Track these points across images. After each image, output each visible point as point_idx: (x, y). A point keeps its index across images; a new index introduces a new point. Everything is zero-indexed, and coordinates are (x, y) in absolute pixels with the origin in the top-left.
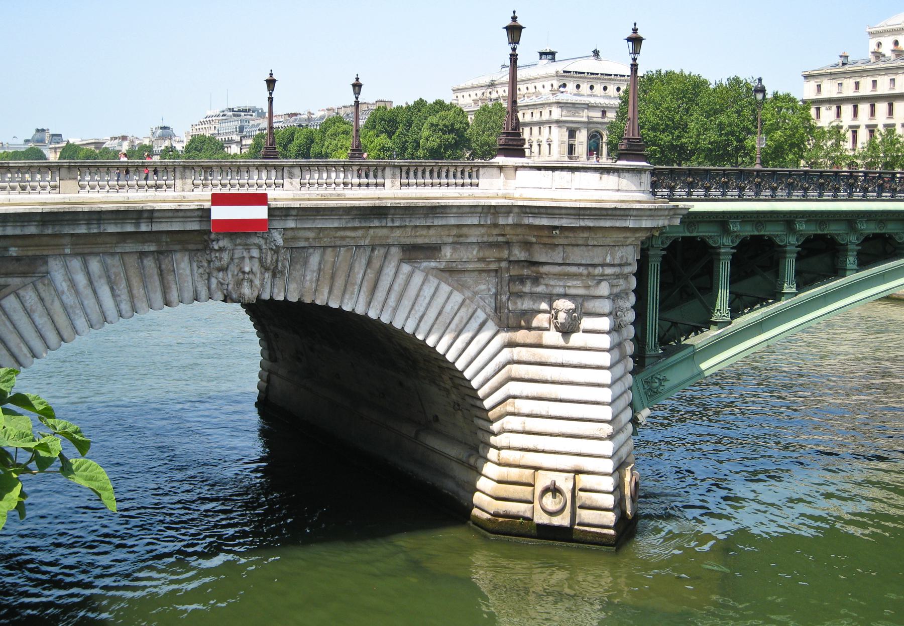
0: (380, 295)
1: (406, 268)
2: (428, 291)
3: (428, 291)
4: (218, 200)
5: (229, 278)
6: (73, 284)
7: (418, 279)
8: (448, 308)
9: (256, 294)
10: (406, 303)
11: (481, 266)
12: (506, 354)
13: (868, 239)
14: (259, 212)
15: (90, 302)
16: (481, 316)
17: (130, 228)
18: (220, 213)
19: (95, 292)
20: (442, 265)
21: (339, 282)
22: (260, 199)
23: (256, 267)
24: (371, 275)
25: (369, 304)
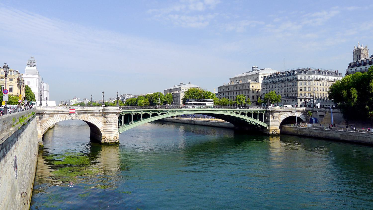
0: (88, 119)
1: (91, 116)
2: (94, 119)
3: (94, 119)
5: (72, 117)
12: (103, 125)
16: (100, 121)
22: (74, 110)
23: (75, 116)
25: (87, 120)
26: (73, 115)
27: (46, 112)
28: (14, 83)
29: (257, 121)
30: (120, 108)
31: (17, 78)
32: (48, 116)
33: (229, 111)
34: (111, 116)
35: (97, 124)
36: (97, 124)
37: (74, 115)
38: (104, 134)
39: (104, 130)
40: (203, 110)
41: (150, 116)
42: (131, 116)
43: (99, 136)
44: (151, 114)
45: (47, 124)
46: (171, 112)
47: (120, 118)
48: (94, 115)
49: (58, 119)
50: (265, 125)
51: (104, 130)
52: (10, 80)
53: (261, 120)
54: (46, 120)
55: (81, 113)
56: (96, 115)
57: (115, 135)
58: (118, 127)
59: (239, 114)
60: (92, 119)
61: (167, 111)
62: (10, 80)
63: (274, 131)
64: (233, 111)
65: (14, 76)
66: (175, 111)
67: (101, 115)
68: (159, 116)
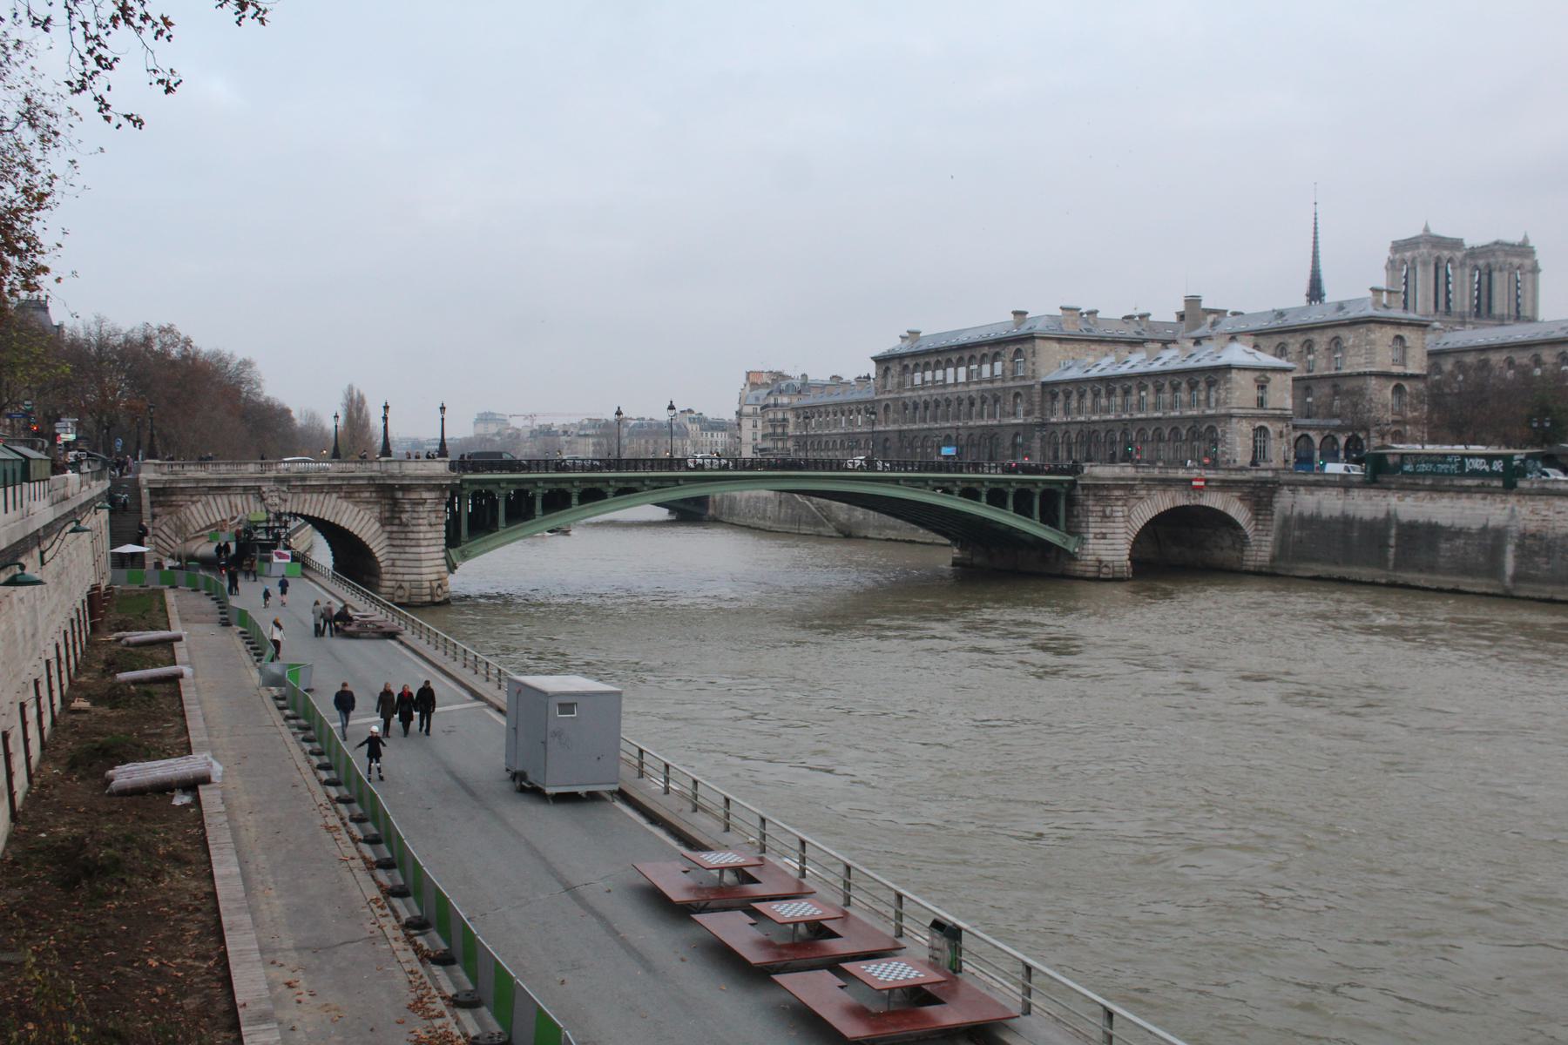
29: (1032, 524)
30: (452, 467)
33: (906, 479)
40: (795, 477)
41: (575, 500)
43: (374, 580)
44: (575, 492)
50: (1071, 546)
53: (1049, 519)
56: (357, 495)
58: (444, 541)
59: (951, 492)
61: (641, 480)
63: (1106, 566)
64: (925, 480)
66: (676, 480)
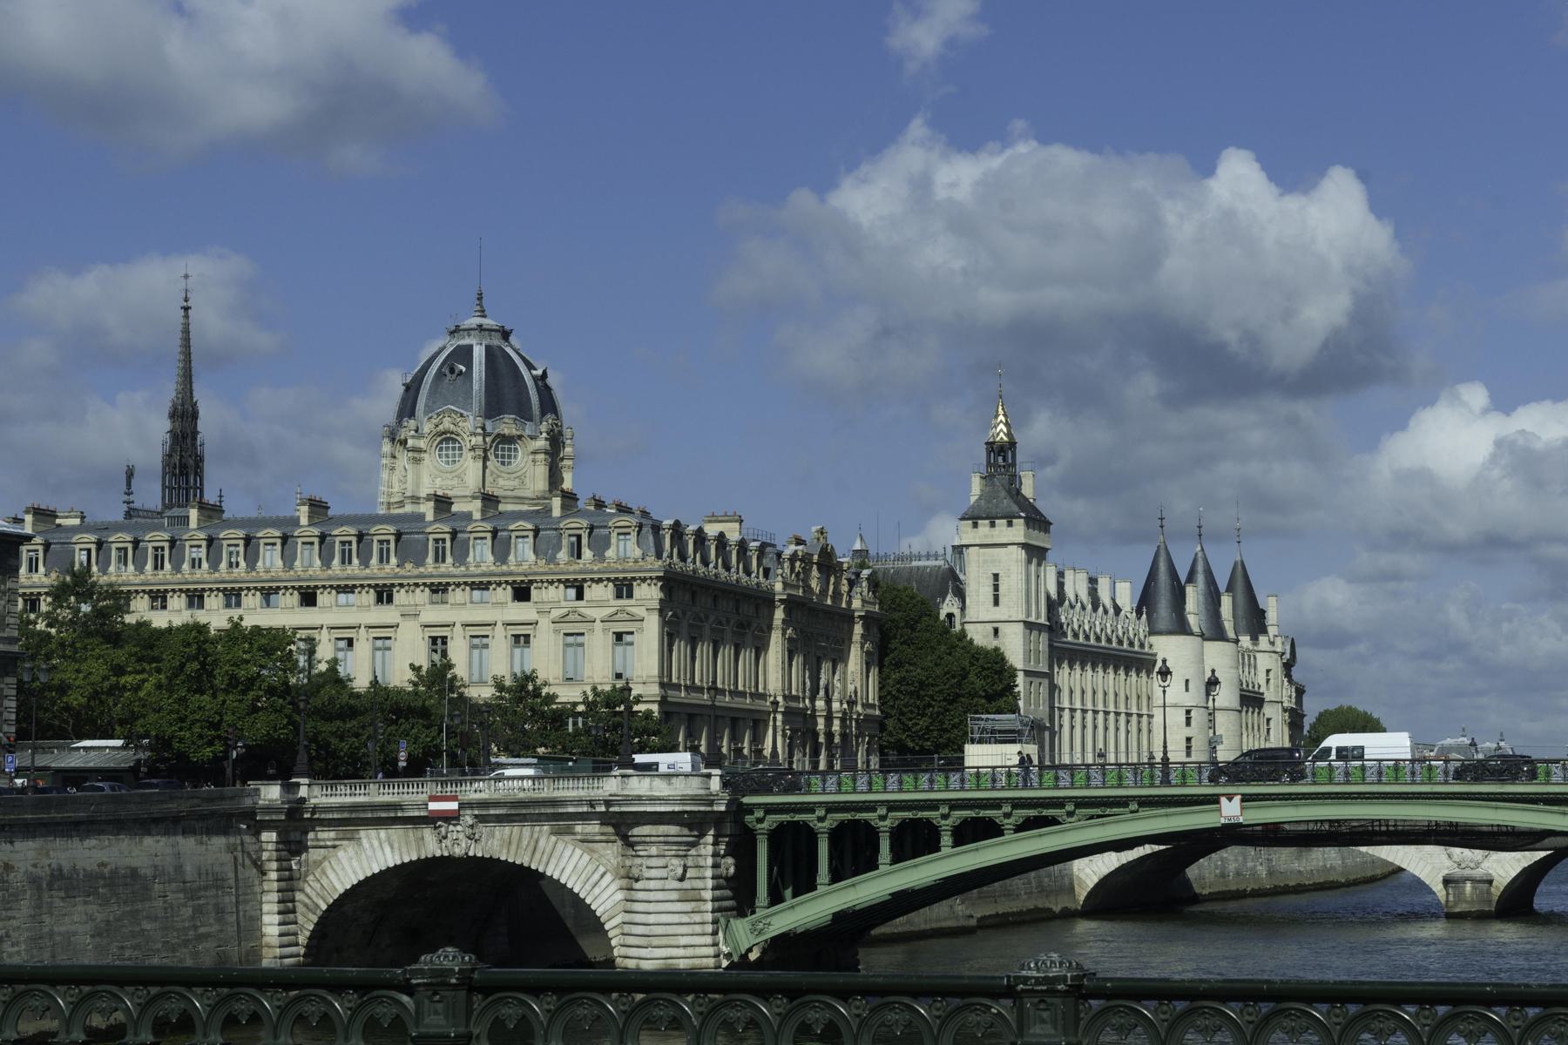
0: (537, 856)
1: (553, 838)
2: (567, 853)
4: (434, 799)
6: (372, 845)
7: (560, 846)
8: (580, 865)
9: (463, 852)
10: (553, 861)
11: (603, 838)
12: (620, 896)
13: (966, 822)
14: (454, 806)
15: (379, 854)
16: (602, 869)
17: (392, 815)
18: (433, 806)
19: (383, 850)
20: (579, 837)
21: (513, 847)
23: (461, 836)
24: (532, 843)
26: (451, 828)
27: (313, 813)
28: (640, 612)
31: (658, 578)
32: (332, 835)
34: (648, 839)
35: (588, 887)
36: (588, 887)
37: (459, 828)
38: (624, 951)
39: (627, 928)
41: (946, 839)
42: (811, 835)
45: (324, 882)
46: (1098, 811)
47: (742, 847)
48: (569, 831)
49: (379, 854)
51: (627, 928)
52: (619, 596)
54: (325, 858)
55: (499, 819)
56: (578, 829)
57: (670, 961)
60: (557, 853)
62: (619, 596)
65: (636, 567)
67: (610, 829)
68: (1008, 836)
